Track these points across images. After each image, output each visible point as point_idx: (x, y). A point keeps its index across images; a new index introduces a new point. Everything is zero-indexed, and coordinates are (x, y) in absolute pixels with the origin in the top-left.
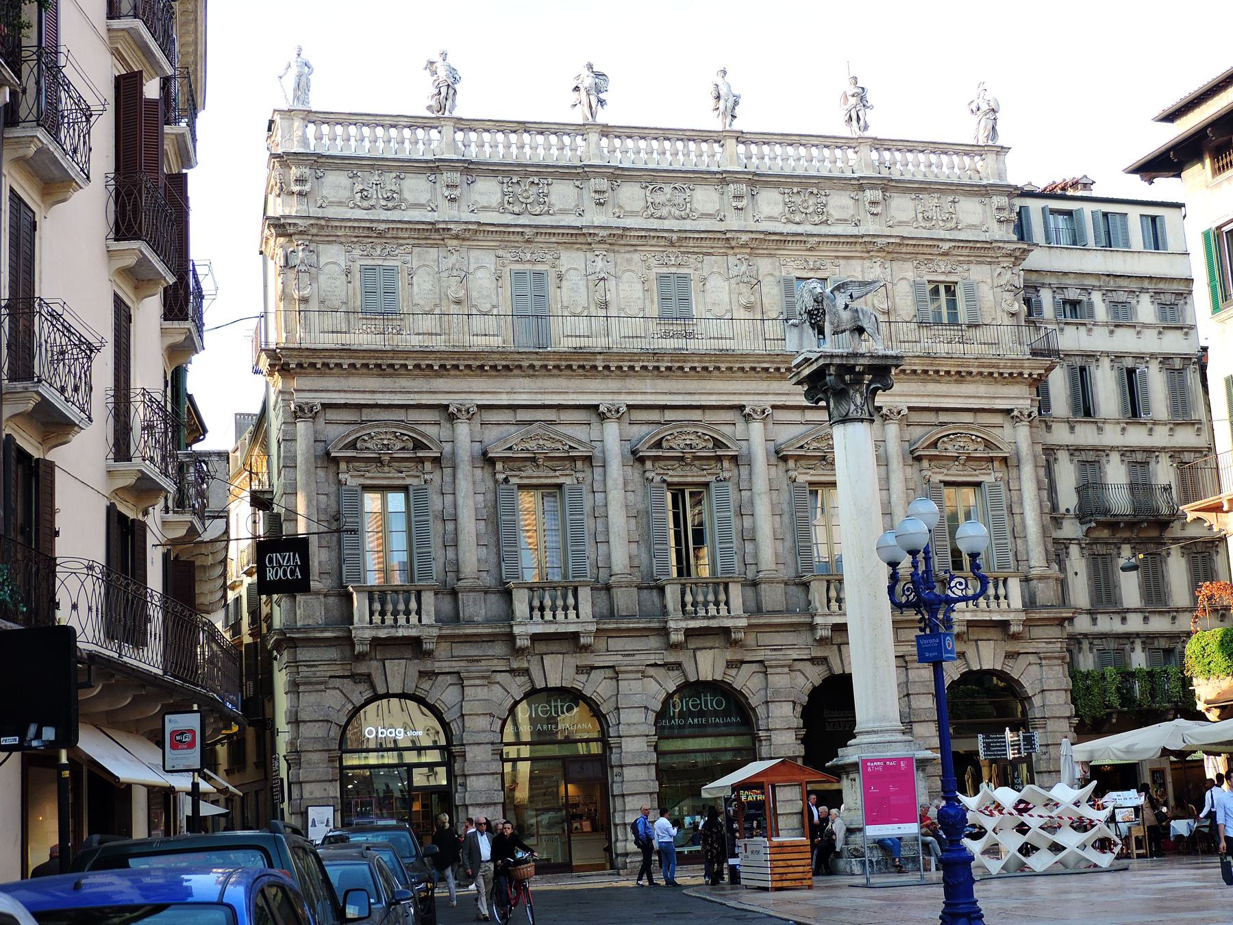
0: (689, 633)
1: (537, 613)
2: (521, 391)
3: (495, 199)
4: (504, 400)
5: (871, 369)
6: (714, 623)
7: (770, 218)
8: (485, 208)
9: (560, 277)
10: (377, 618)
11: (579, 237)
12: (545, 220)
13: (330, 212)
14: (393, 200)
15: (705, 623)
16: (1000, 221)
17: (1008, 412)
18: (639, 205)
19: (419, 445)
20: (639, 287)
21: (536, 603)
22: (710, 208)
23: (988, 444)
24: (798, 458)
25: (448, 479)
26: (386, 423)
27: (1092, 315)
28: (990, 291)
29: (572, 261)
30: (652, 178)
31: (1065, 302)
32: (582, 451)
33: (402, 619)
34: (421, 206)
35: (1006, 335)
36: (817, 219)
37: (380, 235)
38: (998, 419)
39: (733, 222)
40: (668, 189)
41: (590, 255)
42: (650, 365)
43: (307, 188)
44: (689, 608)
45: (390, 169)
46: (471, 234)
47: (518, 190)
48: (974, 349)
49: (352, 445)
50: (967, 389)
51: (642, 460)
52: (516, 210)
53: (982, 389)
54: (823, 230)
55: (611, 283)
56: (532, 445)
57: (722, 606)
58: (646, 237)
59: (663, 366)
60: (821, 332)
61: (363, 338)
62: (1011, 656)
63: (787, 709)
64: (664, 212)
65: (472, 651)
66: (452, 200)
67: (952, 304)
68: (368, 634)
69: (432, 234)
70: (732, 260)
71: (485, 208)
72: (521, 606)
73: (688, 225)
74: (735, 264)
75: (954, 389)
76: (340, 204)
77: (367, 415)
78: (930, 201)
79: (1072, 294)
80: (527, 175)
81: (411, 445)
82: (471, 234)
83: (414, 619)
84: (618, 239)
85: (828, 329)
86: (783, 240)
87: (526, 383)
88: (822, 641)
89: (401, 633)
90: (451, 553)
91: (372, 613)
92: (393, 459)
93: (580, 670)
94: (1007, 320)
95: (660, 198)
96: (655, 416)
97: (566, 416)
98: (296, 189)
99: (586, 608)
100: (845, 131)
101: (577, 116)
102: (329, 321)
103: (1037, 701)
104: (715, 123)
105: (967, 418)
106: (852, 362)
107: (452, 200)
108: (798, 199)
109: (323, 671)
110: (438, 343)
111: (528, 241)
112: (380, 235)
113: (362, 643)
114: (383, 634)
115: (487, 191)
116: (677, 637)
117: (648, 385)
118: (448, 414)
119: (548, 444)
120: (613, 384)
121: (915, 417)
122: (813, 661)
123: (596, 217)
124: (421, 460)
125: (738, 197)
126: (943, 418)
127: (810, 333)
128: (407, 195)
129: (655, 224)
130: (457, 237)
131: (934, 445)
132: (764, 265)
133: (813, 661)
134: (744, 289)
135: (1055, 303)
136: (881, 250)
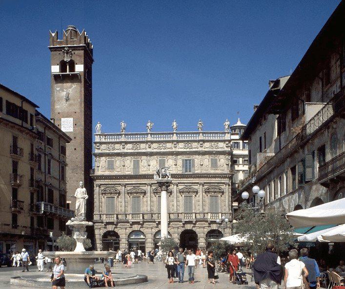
2: (134, 181)
4: (130, 183)
9: (142, 161)
12: (140, 151)
13: (103, 151)
16: (226, 147)
17: (224, 183)
20: (155, 162)
23: (219, 189)
29: (144, 157)
31: (245, 160)
50: (217, 179)
53: (219, 179)
61: (107, 173)
63: (177, 235)
65: (123, 224)
69: (118, 155)
71: (130, 149)
73: (165, 150)
74: (174, 157)
78: (213, 143)
84: (151, 154)
85: (161, 175)
94: (225, 166)
107: (123, 148)
109: (99, 227)
114: (108, 221)
115: (130, 146)
122: (182, 227)
129: (159, 151)
133: (182, 227)
134: (175, 162)
135: (243, 161)
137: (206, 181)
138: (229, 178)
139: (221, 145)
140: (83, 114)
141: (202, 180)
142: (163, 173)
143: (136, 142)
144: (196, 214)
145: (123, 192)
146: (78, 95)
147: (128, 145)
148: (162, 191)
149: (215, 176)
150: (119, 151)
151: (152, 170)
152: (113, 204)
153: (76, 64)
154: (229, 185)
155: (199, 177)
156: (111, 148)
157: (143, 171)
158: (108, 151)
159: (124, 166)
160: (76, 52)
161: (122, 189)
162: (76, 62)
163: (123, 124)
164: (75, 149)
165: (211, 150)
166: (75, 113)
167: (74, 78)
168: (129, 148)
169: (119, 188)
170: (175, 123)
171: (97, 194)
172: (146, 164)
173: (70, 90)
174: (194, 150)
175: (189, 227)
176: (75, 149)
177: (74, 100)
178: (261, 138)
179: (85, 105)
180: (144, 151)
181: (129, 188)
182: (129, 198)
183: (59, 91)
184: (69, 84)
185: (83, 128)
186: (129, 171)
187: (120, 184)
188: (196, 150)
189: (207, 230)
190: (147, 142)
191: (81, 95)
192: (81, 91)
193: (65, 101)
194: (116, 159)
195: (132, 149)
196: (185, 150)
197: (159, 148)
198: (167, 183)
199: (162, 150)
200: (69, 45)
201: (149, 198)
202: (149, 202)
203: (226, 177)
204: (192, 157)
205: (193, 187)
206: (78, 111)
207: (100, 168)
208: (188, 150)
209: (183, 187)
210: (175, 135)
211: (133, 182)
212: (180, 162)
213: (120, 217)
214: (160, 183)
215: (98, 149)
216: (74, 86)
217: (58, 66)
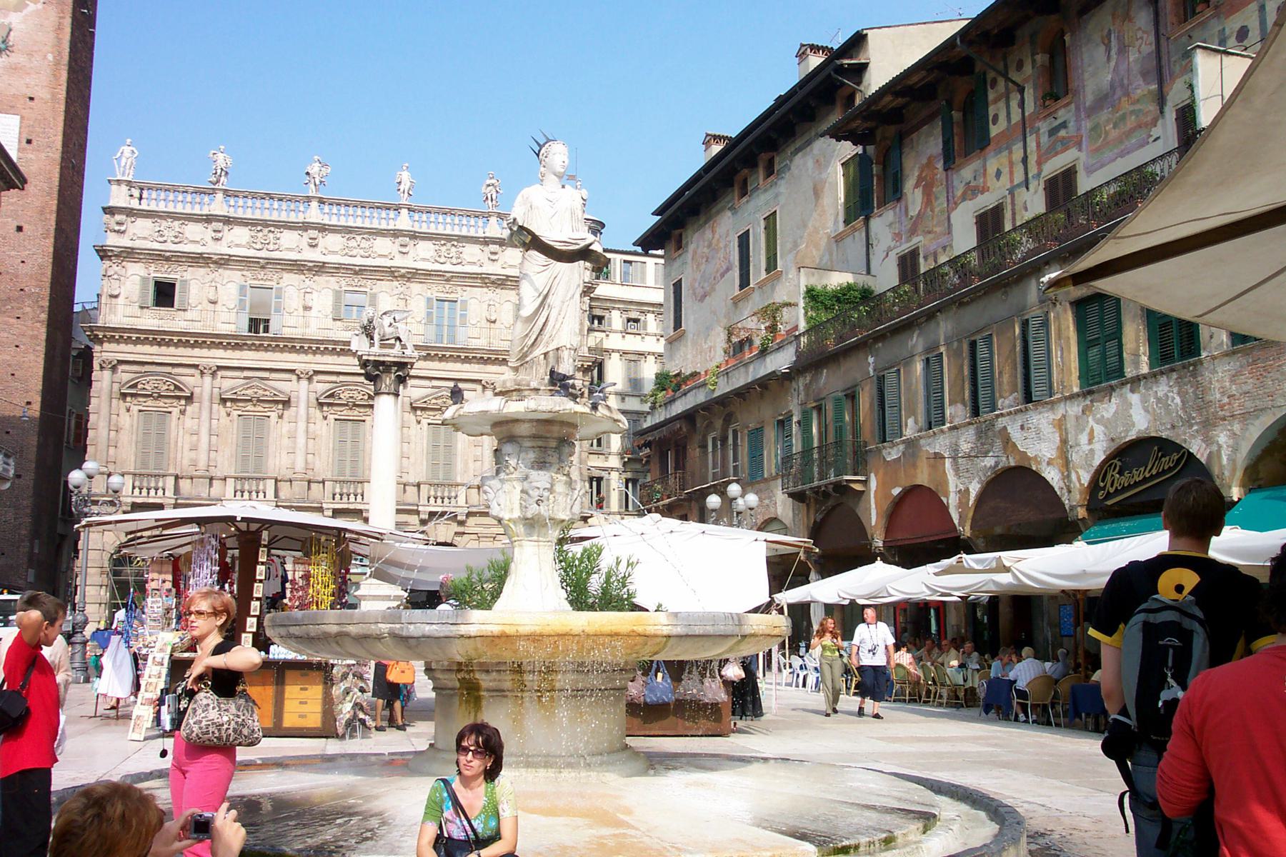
1: (239, 494)
4: (236, 363)
5: (395, 364)
6: (351, 507)
7: (424, 260)
8: (237, 245)
10: (137, 491)
11: (297, 267)
13: (138, 244)
14: (178, 239)
15: (345, 506)
19: (177, 387)
21: (239, 487)
24: (423, 409)
25: (197, 410)
26: (157, 374)
27: (645, 329)
29: (290, 281)
30: (348, 231)
31: (629, 320)
32: (282, 397)
33: (152, 492)
36: (454, 261)
40: (359, 238)
41: (303, 277)
42: (330, 347)
43: (123, 228)
44: (338, 497)
45: (179, 219)
46: (223, 262)
47: (260, 234)
49: (135, 386)
51: (321, 405)
52: (259, 246)
54: (459, 268)
55: (315, 294)
56: (249, 392)
57: (359, 497)
58: (339, 269)
59: (339, 348)
60: (372, 339)
64: (354, 252)
66: (217, 239)
68: (130, 500)
70: (396, 283)
71: (237, 245)
76: (145, 238)
77: (147, 368)
79: (634, 315)
80: (268, 226)
81: (172, 388)
82: (223, 262)
83: (160, 492)
84: (320, 268)
85: (376, 337)
88: (423, 522)
89: (151, 501)
90: (193, 454)
91: (134, 488)
92: (161, 396)
95: (353, 243)
96: (334, 378)
97: (274, 375)
98: (117, 228)
106: (381, 359)
107: (217, 239)
108: (443, 249)
111: (263, 267)
112: (168, 259)
113: (126, 504)
114: (139, 500)
115: (240, 235)
119: (261, 392)
120: (310, 357)
124: (179, 398)
127: (366, 340)
128: (187, 235)
130: (215, 262)
132: (415, 287)
136: (493, 283)
140: (63, 107)
142: (389, 330)
143: (265, 224)
145: (206, 396)
146: (50, 38)
148: (378, 393)
150: (199, 249)
151: (319, 325)
152: (162, 435)
155: (483, 361)
156: (169, 235)
159: (214, 303)
161: (204, 387)
163: (221, 156)
164: (20, 229)
166: (31, 99)
168: (237, 241)
169: (190, 381)
170: (406, 176)
171: (105, 397)
176: (20, 229)
177: (30, 55)
178: (744, 240)
179: (69, 78)
181: (227, 384)
182: (228, 422)
185: (57, 156)
187: (196, 366)
190: (305, 227)
191: (59, 40)
192: (59, 28)
194: (187, 276)
196: (437, 267)
198: (402, 365)
199: (358, 261)
201: (302, 425)
202: (301, 440)
204: (461, 294)
206: (42, 93)
207: (121, 300)
210: (404, 212)
213: (185, 485)
214: (377, 364)
215: (118, 232)
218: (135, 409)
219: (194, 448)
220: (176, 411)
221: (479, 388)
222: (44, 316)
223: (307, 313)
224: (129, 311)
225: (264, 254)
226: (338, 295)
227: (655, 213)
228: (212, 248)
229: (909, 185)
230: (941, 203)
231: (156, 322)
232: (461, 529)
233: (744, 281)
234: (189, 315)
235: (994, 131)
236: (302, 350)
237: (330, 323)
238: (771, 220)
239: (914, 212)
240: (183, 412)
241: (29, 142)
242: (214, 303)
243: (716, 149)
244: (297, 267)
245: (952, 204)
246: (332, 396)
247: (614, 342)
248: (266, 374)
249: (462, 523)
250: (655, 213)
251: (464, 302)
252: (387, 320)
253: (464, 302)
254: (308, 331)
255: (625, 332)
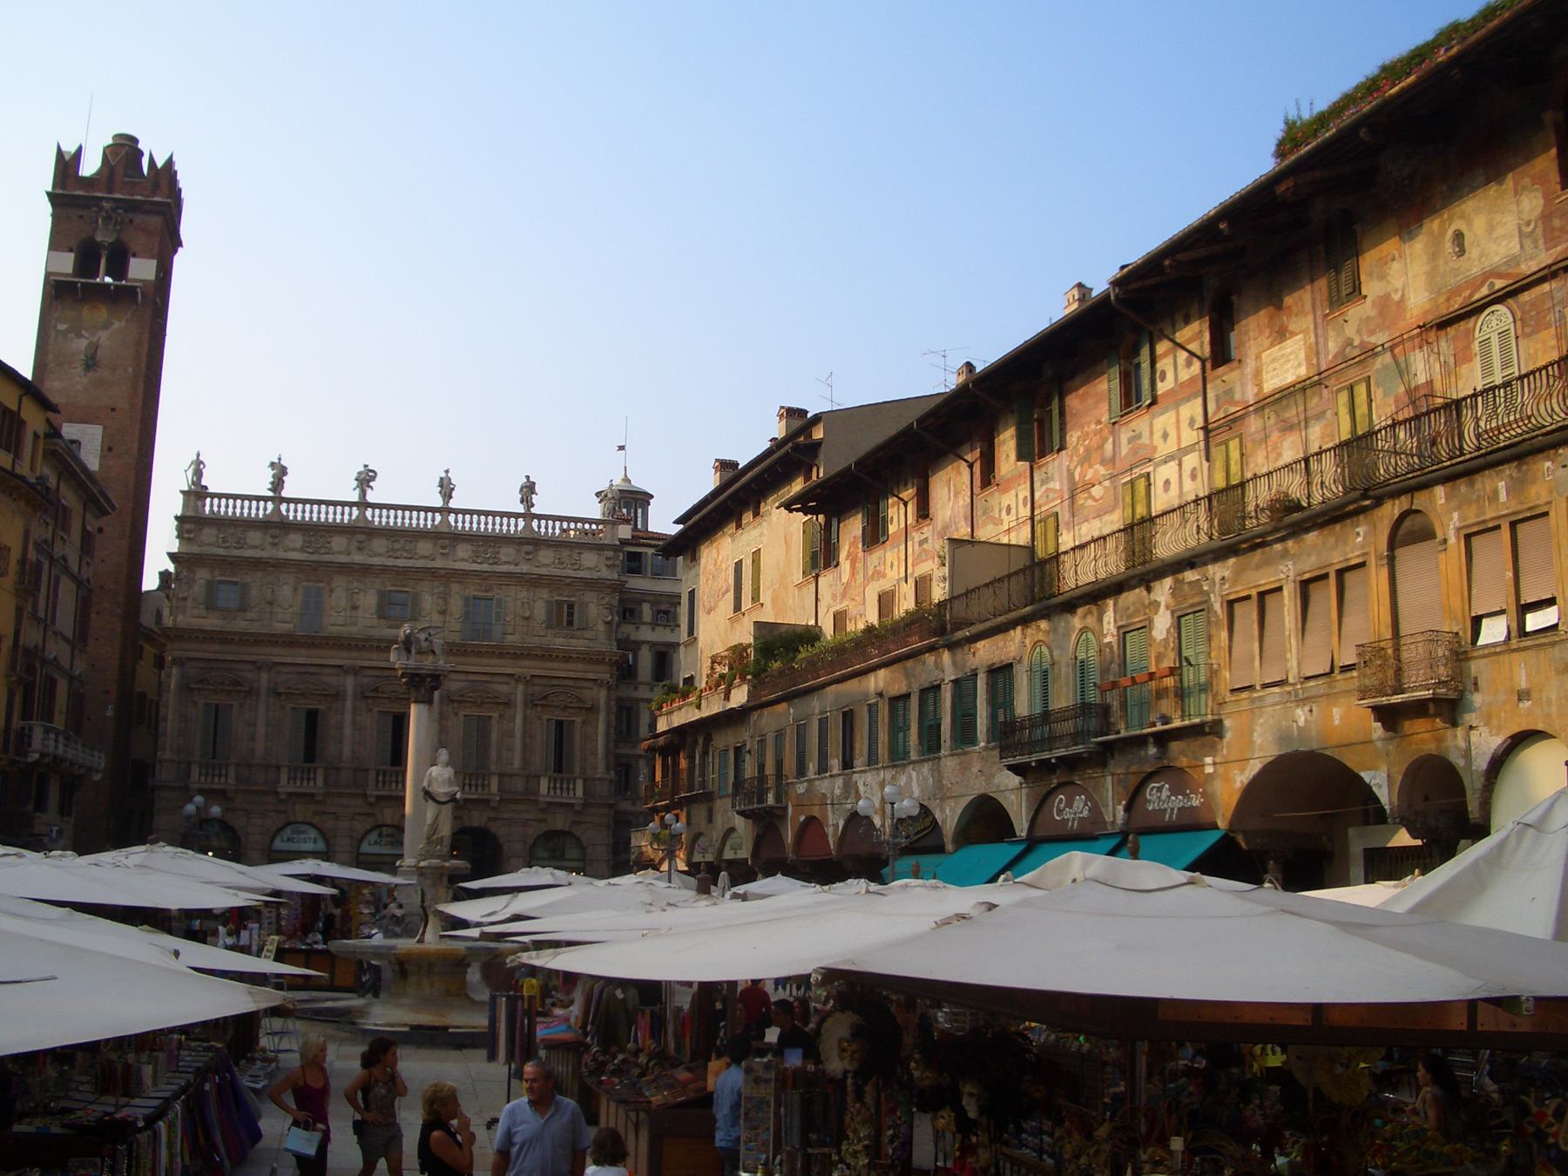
0: (379, 798)
2: (301, 656)
3: (298, 544)
4: (289, 660)
12: (327, 558)
18: (383, 550)
22: (427, 554)
23: (579, 700)
28: (596, 610)
29: (340, 582)
31: (659, 612)
34: (255, 547)
35: (602, 637)
37: (231, 563)
38: (590, 684)
39: (439, 563)
46: (279, 565)
48: (578, 644)
50: (572, 666)
58: (384, 569)
62: (575, 823)
67: (571, 614)
69: (257, 564)
71: (294, 550)
72: (284, 777)
73: (410, 563)
75: (562, 665)
78: (565, 553)
79: (663, 607)
84: (366, 570)
86: (466, 574)
87: (304, 652)
93: (316, 813)
95: (397, 546)
96: (377, 673)
99: (320, 781)
100: (521, 509)
101: (355, 497)
102: (196, 612)
103: (589, 850)
104: (438, 502)
105: (571, 683)
107: (274, 544)
110: (255, 628)
116: (372, 800)
117: (374, 655)
118: (258, 666)
120: (354, 654)
121: (536, 681)
123: (358, 558)
125: (444, 547)
126: (555, 682)
129: (390, 562)
131: (545, 698)
132: (455, 587)
137: (536, 673)
138: (611, 663)
139: (589, 559)
141: (526, 668)
144: (501, 776)
147: (292, 536)
149: (567, 657)
153: (134, 255)
154: (609, 688)
157: (335, 621)
158: (221, 551)
159: (270, 603)
160: (139, 219)
162: (133, 248)
165: (558, 572)
167: (123, 296)
172: (343, 603)
173: (103, 335)
174: (504, 568)
175: (477, 819)
180: (343, 559)
183: (64, 333)
184: (103, 313)
186: (283, 624)
188: (512, 568)
189: (534, 831)
193: (80, 370)
195: (302, 550)
197: (391, 553)
199: (401, 563)
200: (117, 196)
201: (348, 717)
203: (602, 662)
205: (498, 687)
207: (189, 603)
208: (485, 567)
209: (461, 685)
211: (300, 660)
212: (456, 605)
216: (116, 325)
217: (72, 256)
218: (201, 701)
219: (253, 738)
220: (236, 704)
221: (513, 682)
222: (119, 611)
223: (354, 613)
224: (196, 612)
225: (315, 557)
226: (382, 595)
227: (677, 522)
228: (268, 553)
229: (843, 555)
230: (860, 578)
231: (216, 622)
232: (492, 815)
233: (737, 607)
234: (249, 615)
235: (892, 529)
236: (349, 648)
237: (375, 622)
238: (756, 555)
239: (844, 580)
240: (241, 706)
241: (110, 449)
242: (270, 603)
243: (730, 474)
244: (346, 569)
245: (867, 580)
246: (376, 690)
247: (645, 634)
248: (316, 670)
249: (494, 809)
250: (677, 522)
251: (499, 601)
252: (422, 636)
253: (499, 601)
254: (354, 629)
255: (654, 625)
